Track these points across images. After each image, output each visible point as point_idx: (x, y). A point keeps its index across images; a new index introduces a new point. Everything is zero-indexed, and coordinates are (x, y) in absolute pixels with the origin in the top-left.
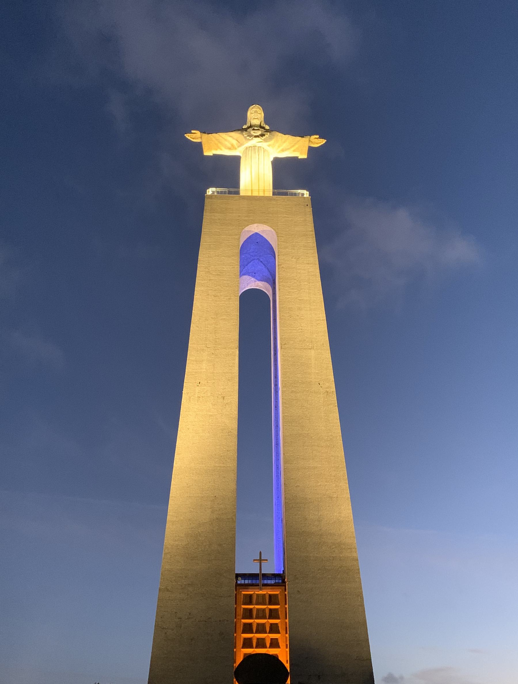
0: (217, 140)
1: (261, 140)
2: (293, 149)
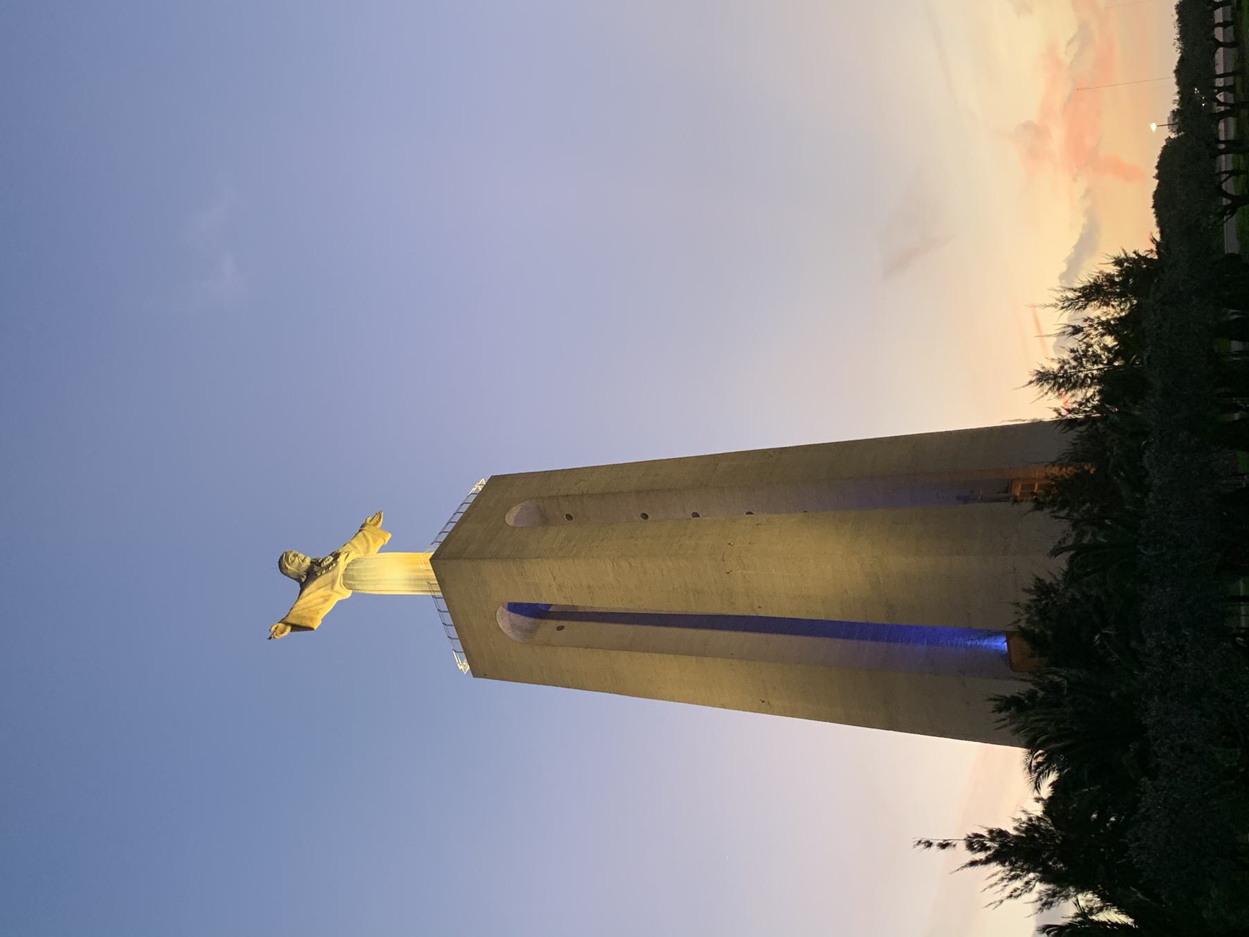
0: (303, 609)
1: (346, 554)
2: (371, 541)
